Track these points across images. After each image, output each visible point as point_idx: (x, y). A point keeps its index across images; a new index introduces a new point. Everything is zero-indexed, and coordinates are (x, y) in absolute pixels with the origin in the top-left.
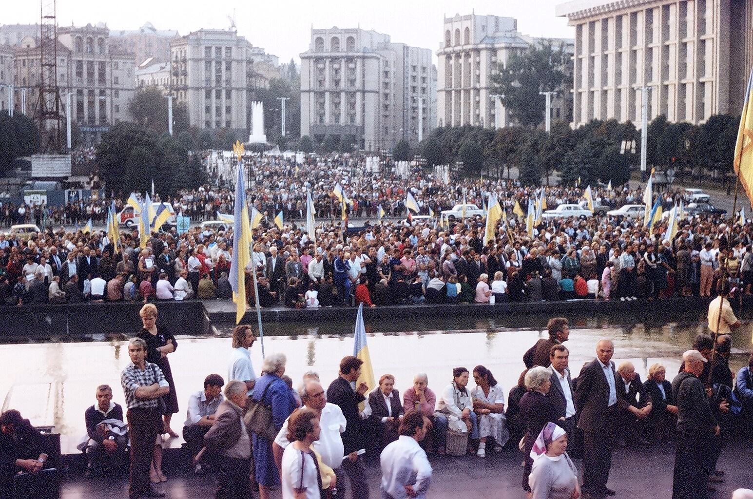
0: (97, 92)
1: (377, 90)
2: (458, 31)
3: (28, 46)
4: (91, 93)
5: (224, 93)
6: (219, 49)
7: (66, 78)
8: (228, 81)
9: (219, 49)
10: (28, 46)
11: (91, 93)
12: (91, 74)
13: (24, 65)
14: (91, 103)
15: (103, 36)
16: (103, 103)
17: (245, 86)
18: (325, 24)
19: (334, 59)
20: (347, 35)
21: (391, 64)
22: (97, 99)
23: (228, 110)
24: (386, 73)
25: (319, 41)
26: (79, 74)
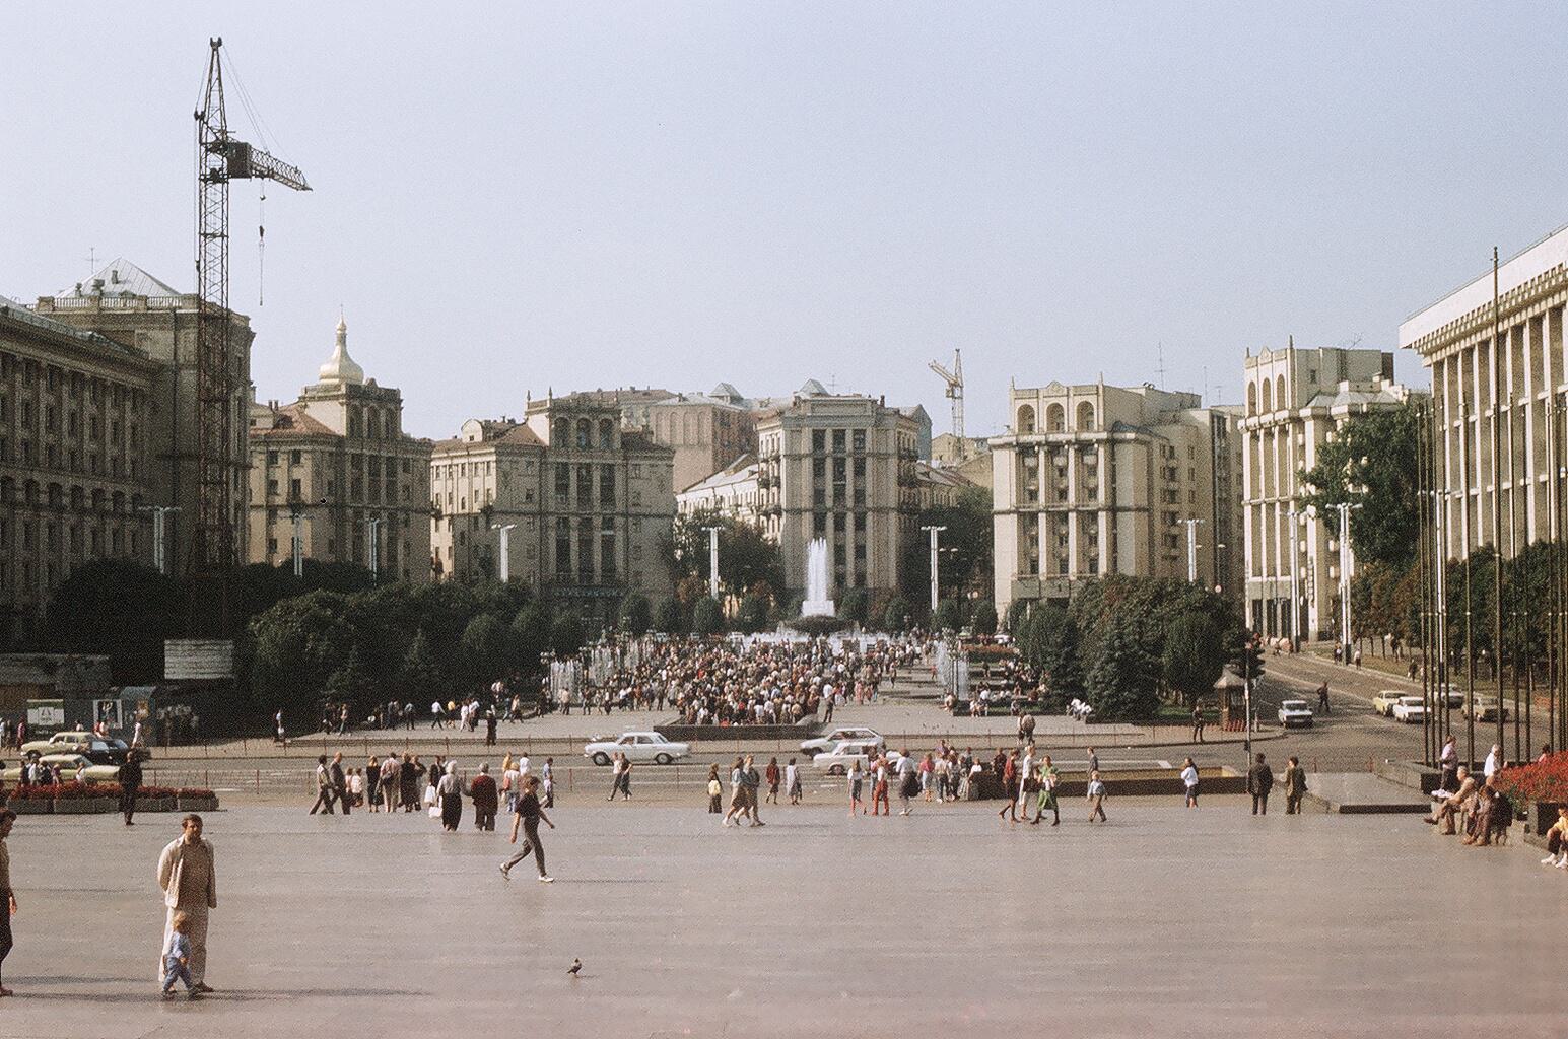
0: (597, 521)
1: (1144, 504)
2: (1267, 382)
3: (472, 438)
4: (586, 524)
5: (850, 520)
6: (839, 437)
7: (536, 497)
8: (859, 495)
9: (839, 437)
10: (472, 438)
11: (586, 524)
12: (585, 489)
13: (463, 474)
14: (586, 543)
15: (609, 417)
16: (608, 543)
17: (893, 503)
18: (1035, 378)
19: (1054, 449)
20: (1079, 399)
21: (1182, 452)
22: (597, 535)
23: (860, 551)
24: (1172, 473)
25: (1026, 413)
26: (562, 488)
